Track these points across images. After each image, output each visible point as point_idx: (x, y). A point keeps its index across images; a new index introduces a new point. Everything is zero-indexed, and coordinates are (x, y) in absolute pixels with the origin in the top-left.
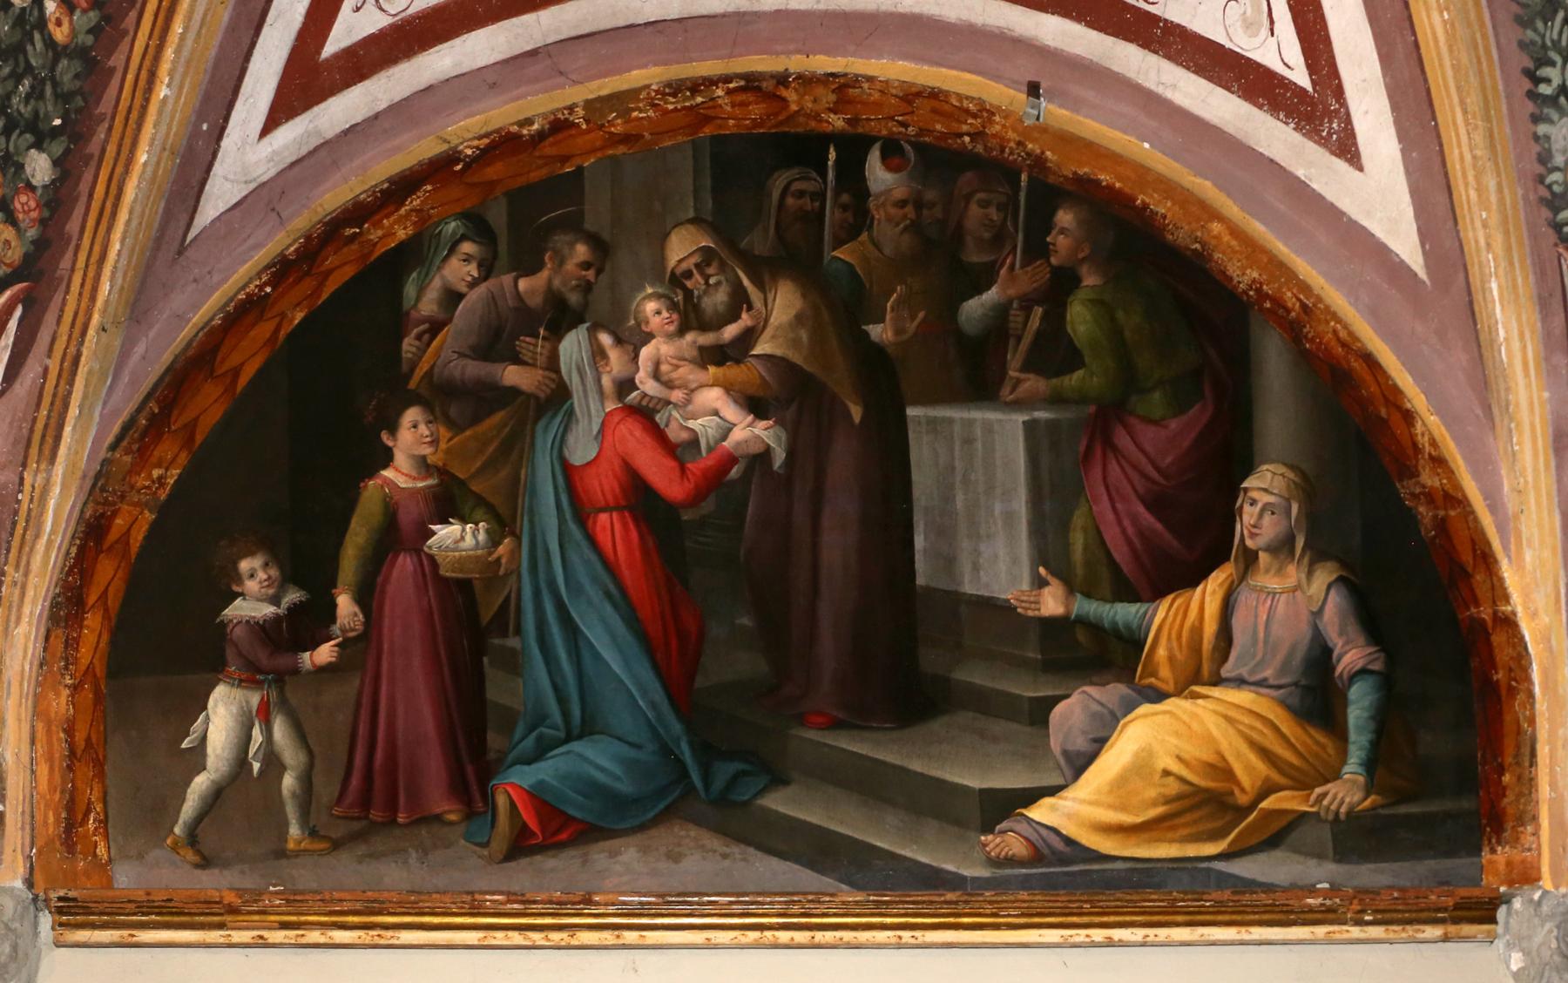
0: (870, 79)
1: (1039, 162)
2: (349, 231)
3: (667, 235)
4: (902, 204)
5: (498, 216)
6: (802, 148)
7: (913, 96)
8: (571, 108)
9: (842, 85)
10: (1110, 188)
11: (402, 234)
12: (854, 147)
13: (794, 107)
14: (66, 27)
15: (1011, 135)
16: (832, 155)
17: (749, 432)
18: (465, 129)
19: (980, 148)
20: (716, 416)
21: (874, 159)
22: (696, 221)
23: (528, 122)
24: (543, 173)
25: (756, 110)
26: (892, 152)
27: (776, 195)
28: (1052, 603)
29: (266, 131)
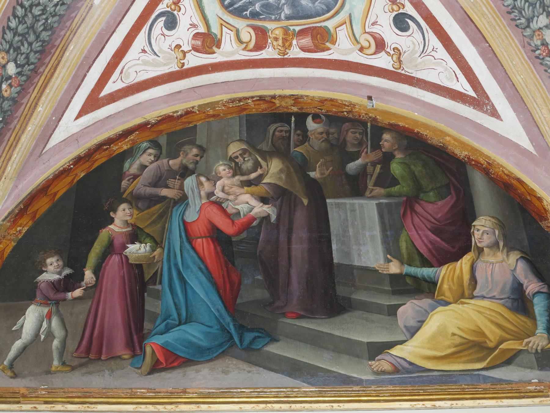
0: (307, 96)
1: (375, 120)
2: (105, 147)
3: (228, 145)
4: (322, 133)
5: (163, 140)
6: (283, 117)
7: (323, 101)
8: (193, 108)
9: (296, 99)
10: (404, 127)
11: (125, 148)
12: (301, 117)
13: (278, 105)
14: (8, 92)
15: (362, 111)
17: (260, 209)
18: (152, 115)
19: (351, 116)
20: (248, 204)
21: (309, 120)
22: (240, 140)
23: (177, 112)
24: (181, 127)
25: (264, 106)
26: (316, 117)
27: (271, 132)
28: (394, 268)
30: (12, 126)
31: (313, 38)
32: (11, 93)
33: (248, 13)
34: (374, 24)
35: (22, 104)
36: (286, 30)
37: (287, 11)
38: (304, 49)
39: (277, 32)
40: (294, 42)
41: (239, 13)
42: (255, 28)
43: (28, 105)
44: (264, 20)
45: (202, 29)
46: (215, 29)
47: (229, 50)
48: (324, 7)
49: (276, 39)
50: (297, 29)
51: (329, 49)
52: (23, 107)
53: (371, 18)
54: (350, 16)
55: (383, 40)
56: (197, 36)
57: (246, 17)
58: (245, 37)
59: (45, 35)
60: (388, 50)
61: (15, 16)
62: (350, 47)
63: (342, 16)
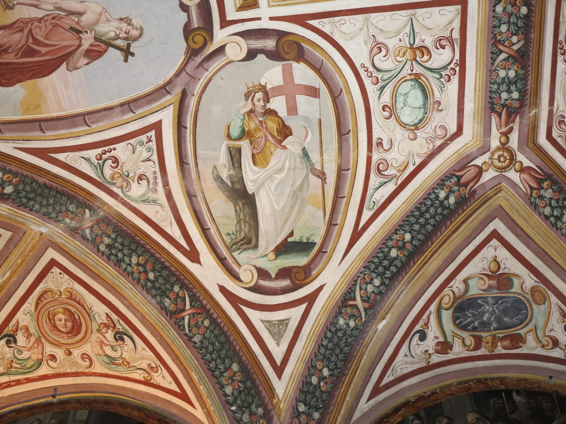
0: (508, 378)
1: (557, 392)
2: (386, 420)
3: (466, 416)
4: (525, 404)
5: (422, 414)
6: (496, 393)
7: (519, 380)
8: (436, 389)
9: (502, 380)
11: (399, 420)
12: (509, 393)
13: (491, 385)
15: (547, 387)
16: (503, 394)
18: (411, 395)
19: (540, 390)
21: (514, 394)
22: (473, 411)
23: (426, 393)
24: (432, 404)
25: (482, 386)
26: (518, 392)
27: (492, 404)
29: (367, 402)
30: (330, 410)
31: (511, 340)
32: (327, 389)
33: (470, 328)
34: (551, 330)
35: (335, 395)
36: (494, 337)
37: (495, 325)
38: (505, 348)
39: (488, 338)
40: (499, 344)
41: (464, 328)
42: (474, 337)
43: (340, 396)
44: (480, 331)
45: (441, 339)
46: (449, 339)
47: (458, 350)
48: (518, 322)
49: (487, 343)
50: (501, 335)
51: (521, 347)
52: (336, 398)
53: (550, 327)
54: (535, 326)
55: (557, 340)
56: (438, 344)
57: (469, 330)
58: (468, 342)
59: (346, 349)
60: (561, 346)
61: (326, 337)
62: (535, 345)
63: (531, 326)
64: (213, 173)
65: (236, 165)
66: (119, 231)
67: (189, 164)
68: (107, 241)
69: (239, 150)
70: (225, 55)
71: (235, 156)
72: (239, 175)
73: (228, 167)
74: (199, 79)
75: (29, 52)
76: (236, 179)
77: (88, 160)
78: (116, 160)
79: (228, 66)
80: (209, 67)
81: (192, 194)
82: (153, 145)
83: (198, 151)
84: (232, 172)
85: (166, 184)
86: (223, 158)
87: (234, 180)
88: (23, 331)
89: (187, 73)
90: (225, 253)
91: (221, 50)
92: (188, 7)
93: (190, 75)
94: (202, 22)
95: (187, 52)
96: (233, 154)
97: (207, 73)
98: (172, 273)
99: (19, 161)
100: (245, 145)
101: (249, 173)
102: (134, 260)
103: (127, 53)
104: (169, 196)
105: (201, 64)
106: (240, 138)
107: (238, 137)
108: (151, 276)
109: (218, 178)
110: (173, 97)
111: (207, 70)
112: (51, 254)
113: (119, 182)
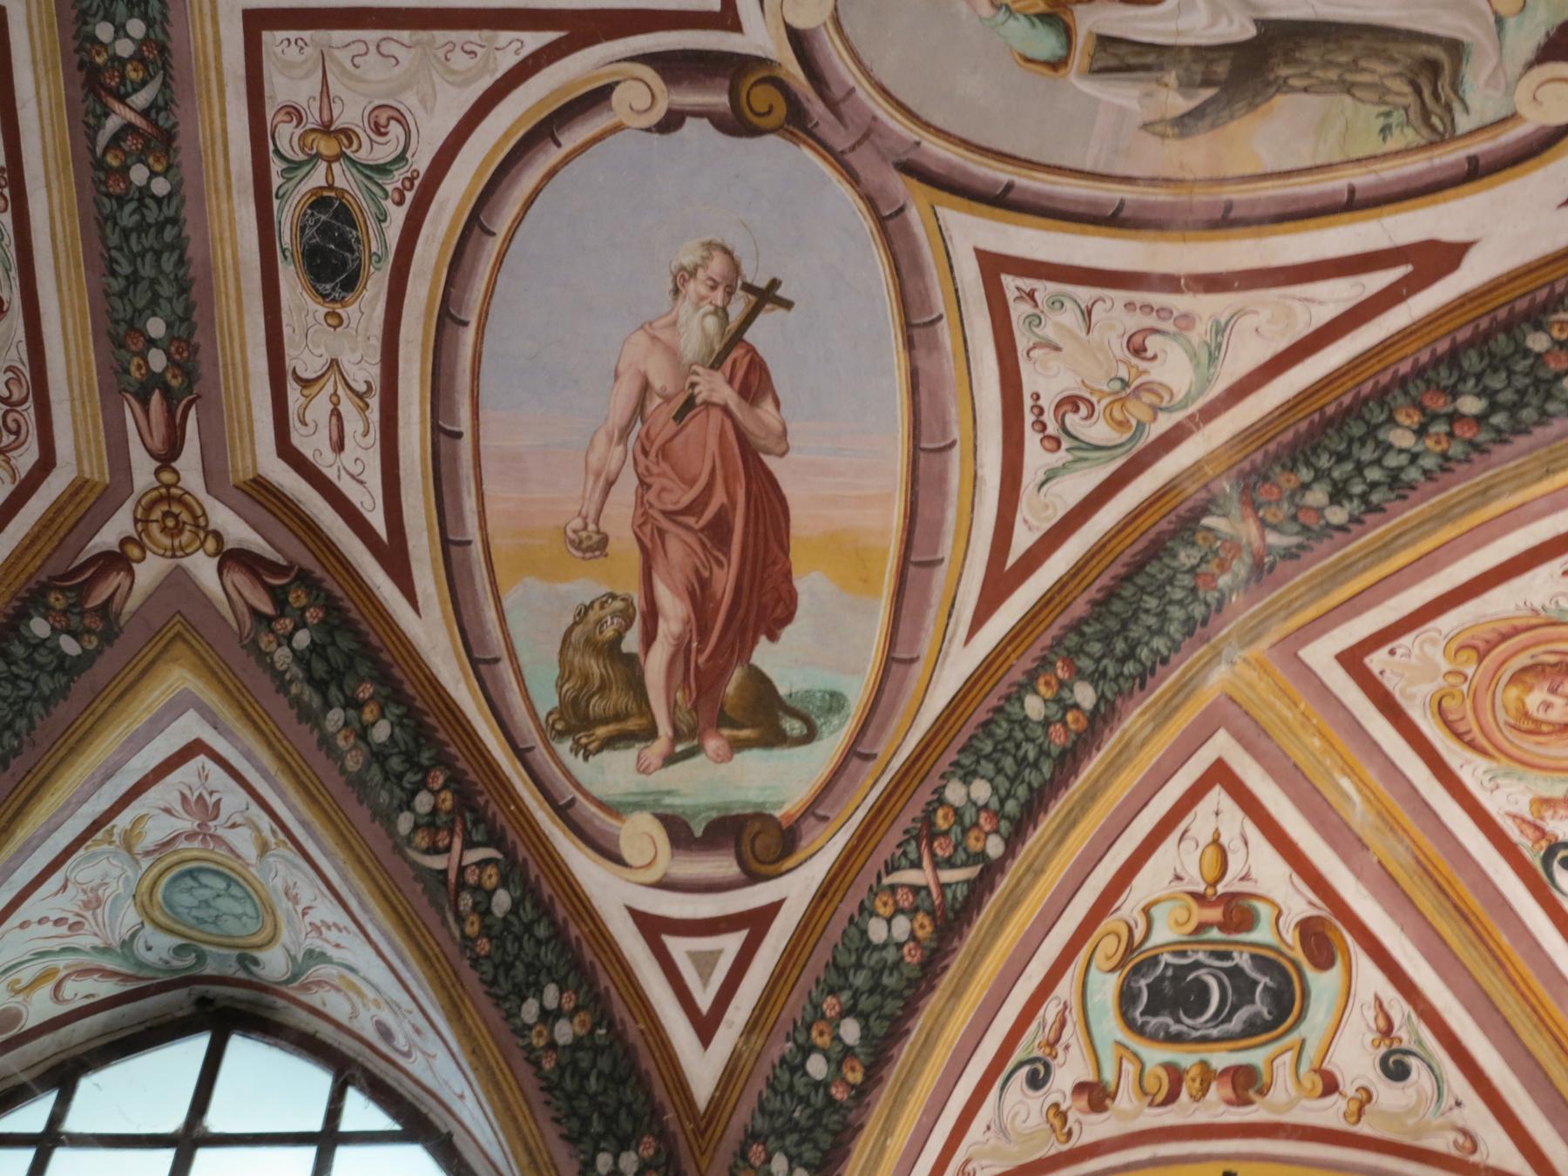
64: (1164, 136)
65: (1150, 59)
66: (1300, 452)
67: (1122, 202)
68: (1317, 496)
69: (1105, 42)
70: (815, 31)
71: (1121, 58)
72: (1187, 56)
73: (1153, 86)
74: (875, 118)
75: (718, 531)
76: (1198, 69)
77: (1051, 475)
78: (1071, 402)
79: (847, 30)
80: (843, 83)
81: (1218, 215)
82: (1045, 289)
83: (1088, 166)
84: (1171, 78)
85: (1170, 283)
86: (1124, 97)
87: (1198, 78)
88: (1549, 813)
89: (853, 148)
90: (1451, 156)
91: (799, 40)
92: (670, 112)
93: (859, 142)
94: (718, 81)
95: (794, 138)
96: (1113, 62)
97: (860, 94)
98: (1481, 340)
99: (1009, 643)
100: (1088, 22)
101: (1184, 23)
102: (1402, 438)
103: (766, 296)
104: (1213, 283)
105: (832, 106)
106: (1068, 33)
107: (1063, 39)
108: (1471, 405)
109: (1184, 124)
110: (916, 202)
111: (852, 91)
112: (1321, 654)
113: (1137, 411)
